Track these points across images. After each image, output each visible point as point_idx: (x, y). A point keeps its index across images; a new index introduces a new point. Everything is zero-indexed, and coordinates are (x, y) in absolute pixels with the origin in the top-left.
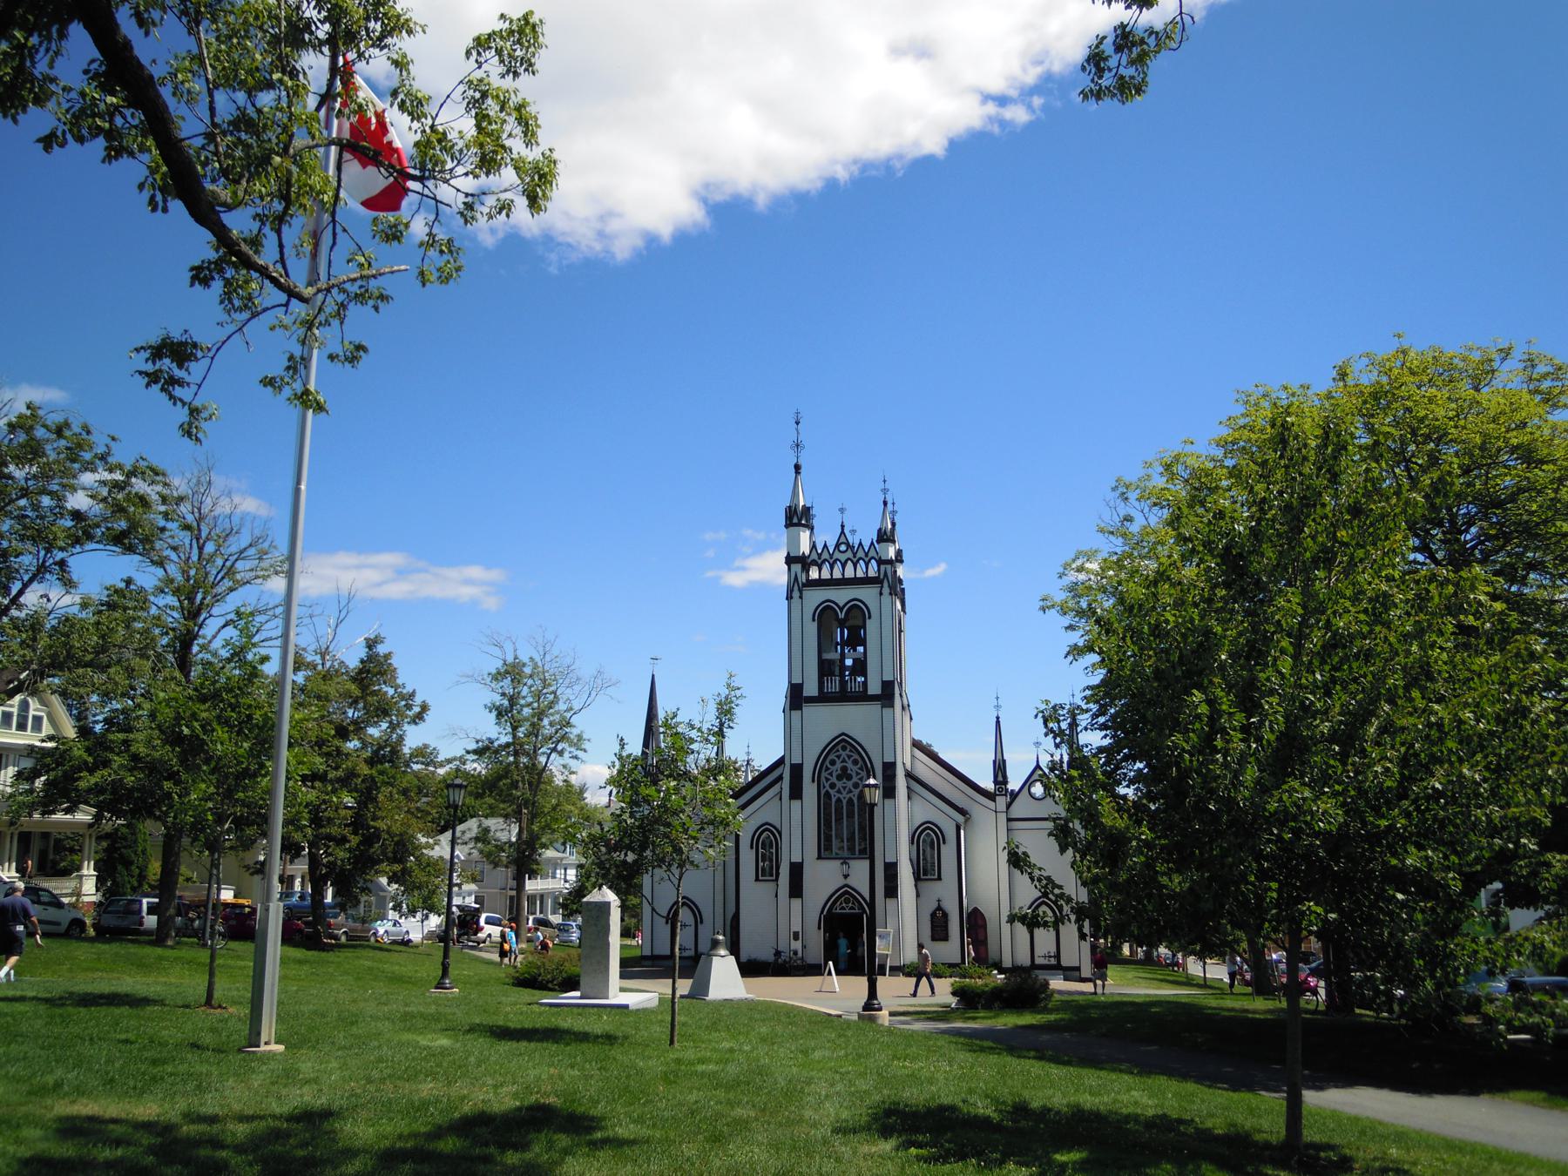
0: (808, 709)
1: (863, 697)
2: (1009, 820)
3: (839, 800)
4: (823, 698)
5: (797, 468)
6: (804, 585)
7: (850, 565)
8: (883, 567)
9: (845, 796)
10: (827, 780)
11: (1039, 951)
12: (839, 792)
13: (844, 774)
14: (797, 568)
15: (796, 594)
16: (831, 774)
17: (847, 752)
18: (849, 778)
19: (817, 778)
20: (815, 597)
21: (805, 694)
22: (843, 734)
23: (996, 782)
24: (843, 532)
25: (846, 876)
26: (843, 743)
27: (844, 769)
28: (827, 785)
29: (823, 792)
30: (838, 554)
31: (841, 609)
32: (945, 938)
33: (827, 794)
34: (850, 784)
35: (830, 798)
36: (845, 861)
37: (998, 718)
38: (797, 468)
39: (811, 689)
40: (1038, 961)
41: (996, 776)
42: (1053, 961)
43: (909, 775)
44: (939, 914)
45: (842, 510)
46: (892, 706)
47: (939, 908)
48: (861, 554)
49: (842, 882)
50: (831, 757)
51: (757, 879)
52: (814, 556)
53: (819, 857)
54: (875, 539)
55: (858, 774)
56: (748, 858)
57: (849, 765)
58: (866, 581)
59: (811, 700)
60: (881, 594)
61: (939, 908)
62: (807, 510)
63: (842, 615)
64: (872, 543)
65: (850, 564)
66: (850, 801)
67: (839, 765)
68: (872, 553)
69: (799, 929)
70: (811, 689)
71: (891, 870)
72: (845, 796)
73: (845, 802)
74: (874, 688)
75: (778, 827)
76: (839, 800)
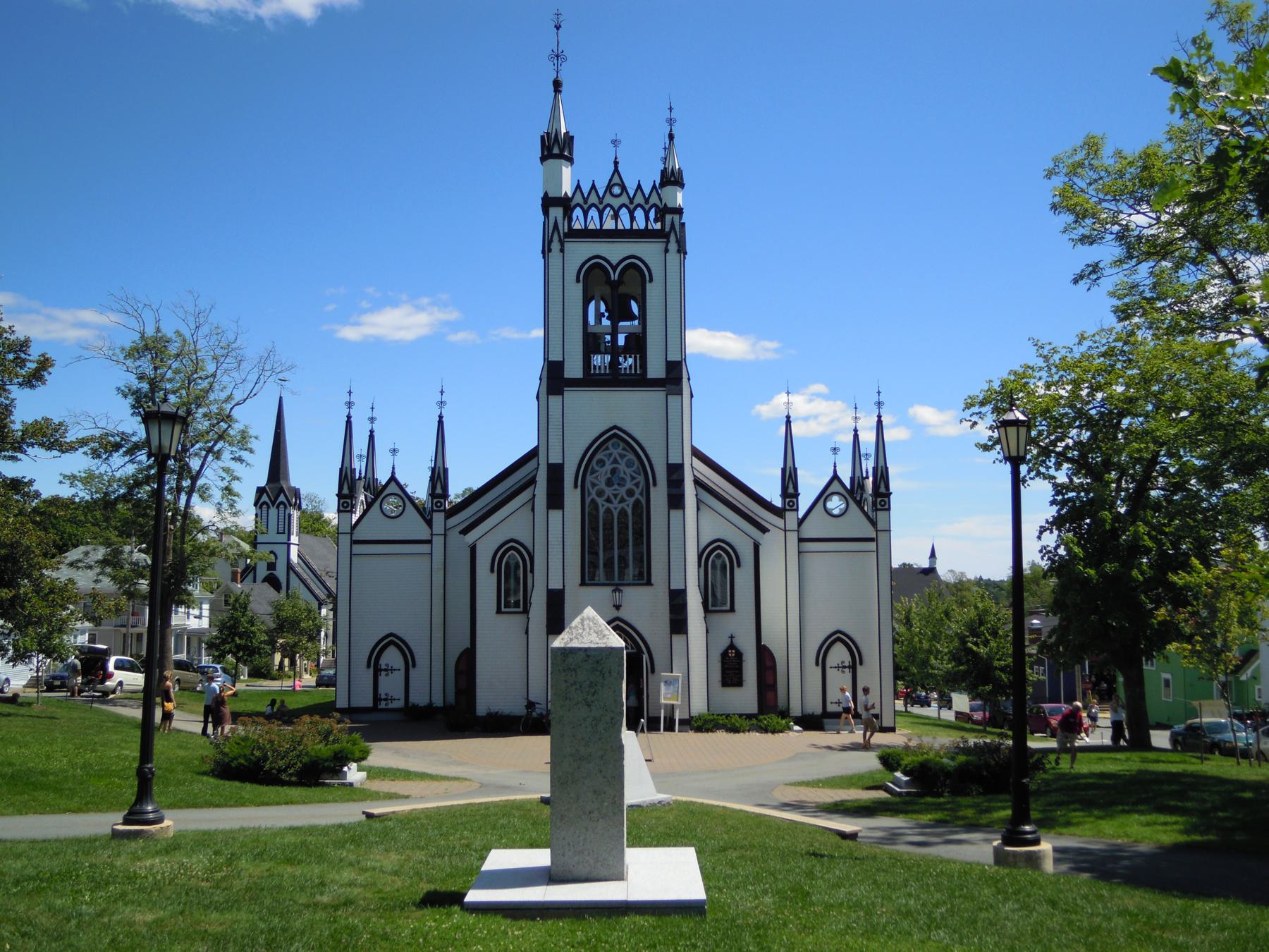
0: (571, 395)
1: (639, 380)
2: (801, 540)
3: (608, 511)
4: (590, 380)
5: (557, 85)
6: (567, 235)
9: (616, 507)
10: (594, 485)
11: (833, 695)
12: (608, 500)
14: (557, 212)
15: (556, 246)
17: (620, 450)
18: (622, 482)
19: (581, 482)
20: (580, 252)
21: (566, 375)
22: (615, 427)
24: (616, 170)
25: (618, 607)
26: (615, 438)
28: (593, 492)
30: (608, 199)
31: (614, 268)
33: (593, 501)
38: (557, 85)
39: (574, 369)
40: (831, 708)
43: (697, 482)
44: (732, 653)
45: (615, 143)
46: (681, 394)
47: (732, 646)
50: (598, 457)
51: (499, 611)
52: (578, 199)
53: (583, 583)
55: (633, 478)
56: (487, 584)
57: (622, 466)
58: (645, 234)
59: (574, 383)
60: (667, 251)
61: (732, 646)
62: (569, 139)
64: (654, 187)
65: (624, 212)
66: (623, 513)
67: (608, 467)
68: (654, 199)
70: (574, 369)
71: (677, 600)
72: (616, 507)
73: (616, 514)
74: (656, 369)
75: (529, 546)
76: (608, 511)
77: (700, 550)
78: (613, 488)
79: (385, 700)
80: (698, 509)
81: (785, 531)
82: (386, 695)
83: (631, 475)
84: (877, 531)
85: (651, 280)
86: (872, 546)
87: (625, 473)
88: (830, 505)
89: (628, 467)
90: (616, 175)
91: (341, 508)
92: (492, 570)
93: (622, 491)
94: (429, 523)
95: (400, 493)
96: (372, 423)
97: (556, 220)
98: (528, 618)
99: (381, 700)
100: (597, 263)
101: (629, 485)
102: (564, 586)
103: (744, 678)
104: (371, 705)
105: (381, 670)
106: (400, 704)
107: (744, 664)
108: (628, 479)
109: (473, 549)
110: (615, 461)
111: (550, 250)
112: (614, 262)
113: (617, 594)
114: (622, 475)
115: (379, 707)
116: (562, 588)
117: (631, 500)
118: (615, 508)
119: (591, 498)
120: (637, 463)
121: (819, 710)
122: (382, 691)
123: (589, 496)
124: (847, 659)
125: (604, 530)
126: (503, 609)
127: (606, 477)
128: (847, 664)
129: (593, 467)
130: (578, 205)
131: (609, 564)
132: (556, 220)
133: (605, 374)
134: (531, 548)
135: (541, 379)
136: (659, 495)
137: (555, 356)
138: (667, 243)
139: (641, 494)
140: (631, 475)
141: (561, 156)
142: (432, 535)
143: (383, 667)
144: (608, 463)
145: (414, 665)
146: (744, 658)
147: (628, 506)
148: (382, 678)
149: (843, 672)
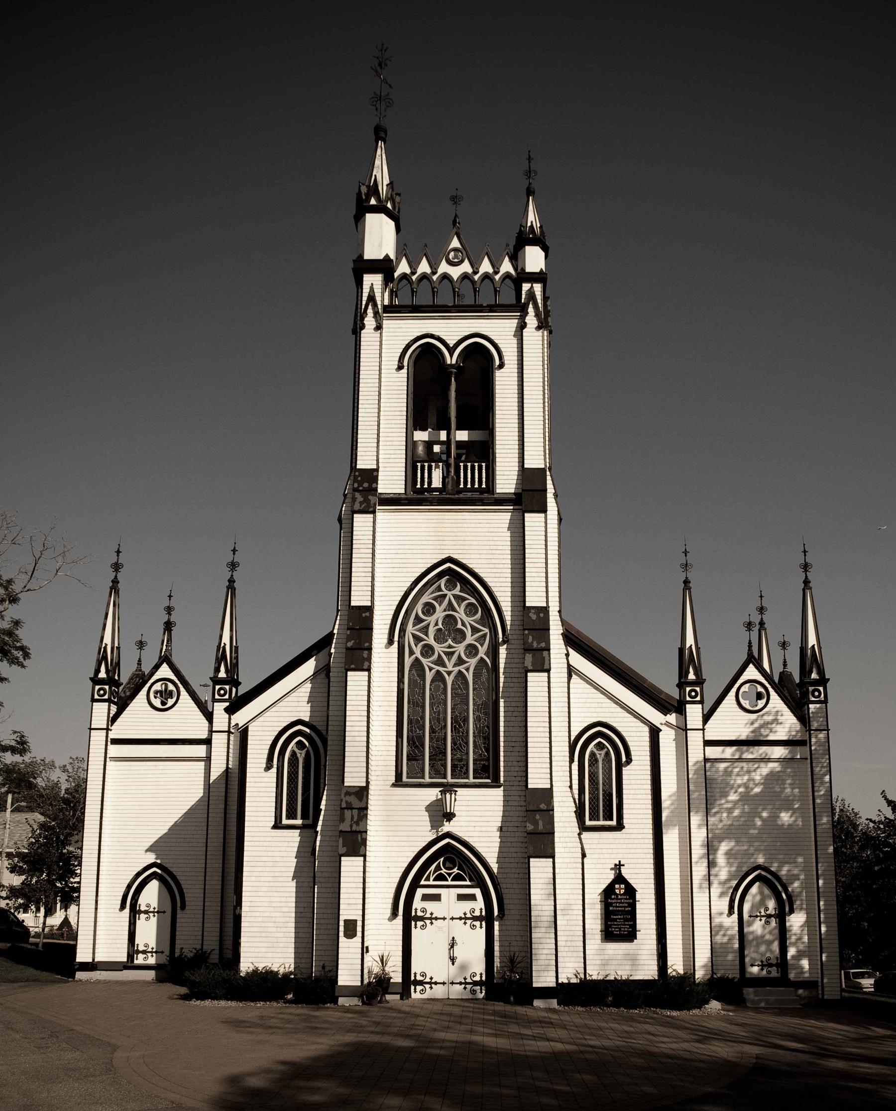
0: (385, 517)
3: (439, 677)
10: (417, 639)
12: (440, 662)
16: (425, 630)
17: (457, 591)
22: (450, 560)
27: (450, 620)
31: (451, 351)
32: (630, 935)
33: (417, 664)
34: (460, 648)
35: (423, 676)
44: (620, 889)
47: (619, 878)
50: (426, 598)
51: (277, 826)
53: (398, 782)
55: (475, 630)
57: (460, 613)
67: (440, 613)
73: (449, 680)
76: (439, 677)
77: (572, 738)
78: (446, 644)
79: (144, 952)
80: (570, 677)
83: (472, 626)
87: (463, 624)
89: (467, 615)
91: (96, 697)
93: (460, 648)
94: (209, 716)
99: (138, 952)
100: (428, 343)
101: (470, 639)
102: (368, 782)
103: (638, 927)
104: (124, 958)
105: (140, 912)
107: (638, 906)
108: (468, 632)
110: (450, 606)
112: (451, 343)
114: (459, 626)
116: (364, 784)
117: (473, 662)
119: (414, 656)
126: (285, 821)
127: (437, 627)
129: (417, 615)
131: (438, 754)
134: (324, 733)
135: (345, 496)
139: (487, 654)
140: (472, 626)
142: (211, 731)
143: (143, 908)
146: (638, 897)
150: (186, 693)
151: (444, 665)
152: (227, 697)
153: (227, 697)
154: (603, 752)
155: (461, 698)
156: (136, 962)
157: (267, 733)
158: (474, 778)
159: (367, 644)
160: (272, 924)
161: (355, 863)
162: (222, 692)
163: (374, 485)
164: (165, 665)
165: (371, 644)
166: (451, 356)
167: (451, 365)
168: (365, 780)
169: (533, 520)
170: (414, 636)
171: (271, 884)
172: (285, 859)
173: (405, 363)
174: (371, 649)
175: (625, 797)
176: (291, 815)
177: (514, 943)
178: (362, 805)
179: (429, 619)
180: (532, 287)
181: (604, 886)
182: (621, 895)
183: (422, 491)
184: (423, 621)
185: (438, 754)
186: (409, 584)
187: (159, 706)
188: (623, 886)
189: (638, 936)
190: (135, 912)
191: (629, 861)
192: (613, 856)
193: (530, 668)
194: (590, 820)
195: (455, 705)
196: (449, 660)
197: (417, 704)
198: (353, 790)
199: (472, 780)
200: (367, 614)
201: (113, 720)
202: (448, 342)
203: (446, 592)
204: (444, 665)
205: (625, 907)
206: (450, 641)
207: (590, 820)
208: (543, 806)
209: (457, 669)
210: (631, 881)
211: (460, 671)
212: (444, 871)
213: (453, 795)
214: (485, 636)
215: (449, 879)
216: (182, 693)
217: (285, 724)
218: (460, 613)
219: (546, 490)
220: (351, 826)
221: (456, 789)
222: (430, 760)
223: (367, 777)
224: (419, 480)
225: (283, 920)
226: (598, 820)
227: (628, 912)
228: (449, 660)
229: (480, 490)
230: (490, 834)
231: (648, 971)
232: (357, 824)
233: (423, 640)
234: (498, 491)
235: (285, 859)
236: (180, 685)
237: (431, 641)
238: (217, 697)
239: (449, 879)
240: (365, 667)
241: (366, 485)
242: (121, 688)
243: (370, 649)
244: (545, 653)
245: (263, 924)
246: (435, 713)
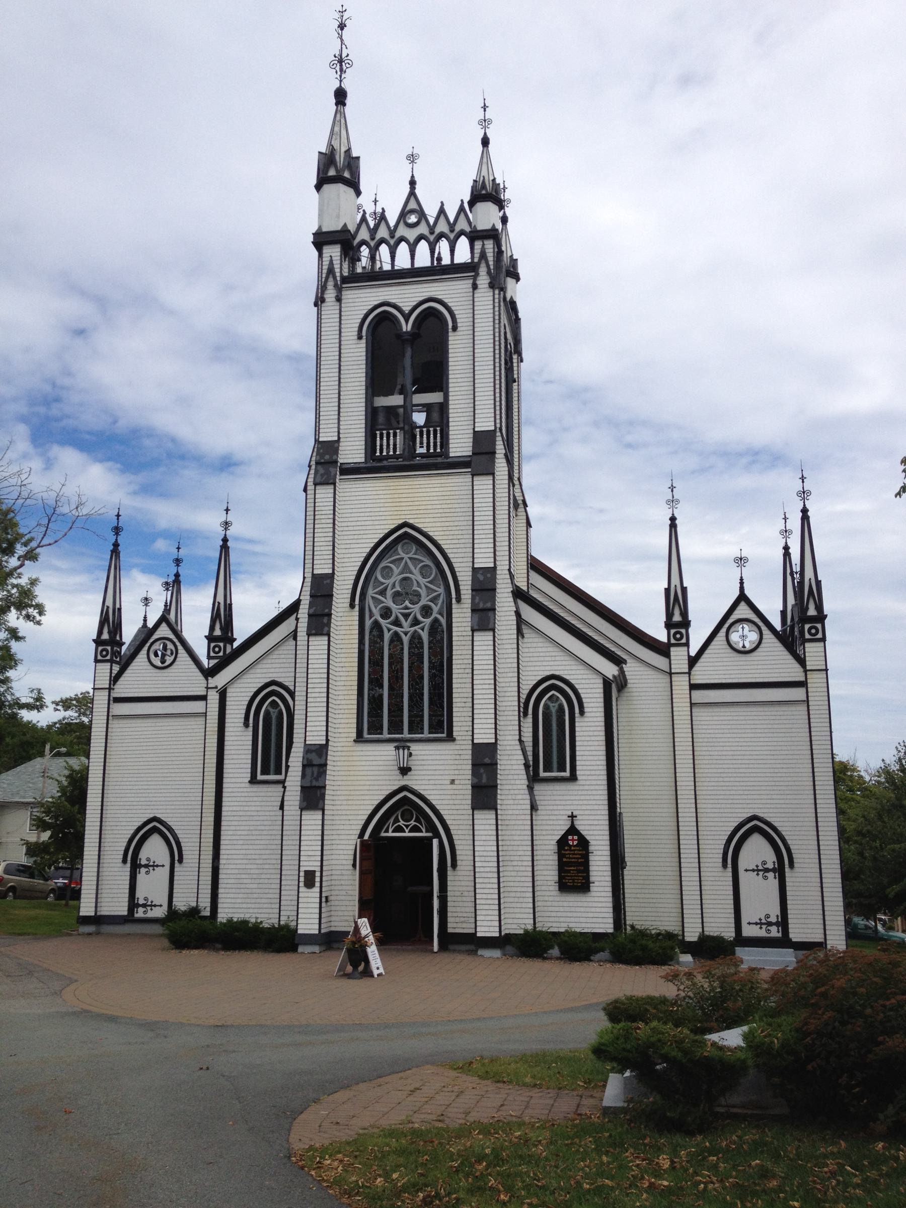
2: (693, 687)
3: (396, 638)
5: (341, 96)
6: (345, 280)
7: (423, 247)
8: (478, 245)
12: (397, 623)
13: (406, 593)
14: (333, 252)
15: (330, 294)
16: (383, 593)
23: (669, 625)
24: (412, 194)
25: (405, 771)
29: (368, 623)
30: (402, 231)
31: (407, 317)
33: (376, 625)
36: (402, 745)
37: (673, 519)
40: (748, 931)
41: (669, 614)
42: (775, 932)
43: (518, 594)
44: (573, 840)
45: (412, 158)
48: (442, 227)
49: (397, 782)
51: (253, 780)
52: (364, 234)
54: (467, 198)
57: (416, 576)
60: (475, 287)
63: (407, 327)
64: (462, 209)
66: (416, 640)
67: (396, 577)
68: (462, 225)
69: (314, 866)
73: (406, 640)
75: (291, 686)
76: (396, 638)
79: (144, 906)
80: (520, 633)
81: (671, 674)
82: (146, 899)
84: (806, 671)
85: (455, 328)
86: (797, 694)
88: (735, 637)
90: (412, 199)
91: (99, 658)
92: (246, 725)
93: (416, 609)
95: (172, 636)
96: (178, 565)
97: (331, 262)
98: (284, 787)
99: (138, 906)
100: (384, 312)
101: (424, 601)
102: (327, 740)
103: (592, 879)
104: (123, 910)
105: (141, 866)
106: (159, 913)
107: (591, 858)
108: (423, 592)
109: (223, 694)
110: (406, 569)
111: (323, 300)
112: (407, 309)
113: (401, 751)
114: (415, 588)
115: (136, 915)
117: (428, 621)
118: (406, 634)
119: (373, 619)
120: (434, 570)
121: (729, 934)
122: (140, 895)
123: (371, 617)
124: (771, 859)
125: (390, 664)
126: (260, 777)
128: (770, 866)
129: (376, 578)
130: (363, 243)
131: (395, 710)
132: (331, 262)
133: (395, 457)
135: (310, 466)
136: (462, 617)
137: (327, 435)
138: (475, 278)
141: (338, 179)
142: (207, 688)
143: (144, 862)
144: (396, 571)
145: (181, 861)
146: (591, 848)
147: (423, 629)
148: (141, 876)
149: (765, 878)
150: (184, 651)
151: (400, 626)
152: (221, 654)
153: (221, 654)
154: (556, 705)
155: (416, 658)
156: (136, 915)
157: (243, 694)
158: (430, 733)
159: (327, 611)
160: (247, 876)
161: (314, 817)
162: (217, 649)
163: (334, 457)
164: (164, 625)
165: (331, 609)
166: (407, 322)
167: (407, 332)
168: (324, 738)
169: (483, 484)
170: (373, 597)
171: (247, 837)
172: (260, 813)
173: (364, 333)
174: (331, 614)
175: (577, 748)
176: (265, 771)
177: (466, 894)
178: (322, 762)
179: (387, 581)
180: (483, 245)
181: (558, 837)
182: (573, 846)
183: (381, 459)
184: (383, 584)
185: (395, 710)
186: (368, 550)
187: (159, 664)
188: (576, 837)
189: (591, 889)
190: (135, 867)
191: (581, 812)
192: (566, 807)
193: (476, 627)
194: (545, 771)
195: (413, 663)
196: (406, 620)
197: (376, 663)
198: (314, 748)
199: (426, 735)
200: (328, 581)
201: (115, 679)
202: (404, 309)
203: (402, 555)
204: (400, 626)
205: (578, 858)
206: (407, 603)
207: (545, 771)
208: (487, 760)
209: (413, 629)
210: (583, 833)
211: (415, 631)
212: (402, 823)
213: (406, 751)
214: (439, 595)
215: (407, 831)
216: (179, 651)
217: (260, 685)
218: (416, 576)
219: (494, 453)
220: (311, 782)
221: (408, 744)
222: (389, 717)
223: (327, 736)
224: (378, 447)
225: (257, 871)
226: (551, 771)
227: (581, 864)
228: (406, 620)
229: (435, 455)
230: (444, 787)
231: (604, 923)
232: (317, 779)
233: (383, 602)
234: (451, 455)
235: (260, 813)
236: (178, 644)
237: (389, 603)
238: (212, 654)
239: (407, 831)
240: (325, 632)
241: (327, 457)
242: (124, 648)
243: (329, 615)
244: (491, 614)
245: (238, 876)
246: (393, 671)
